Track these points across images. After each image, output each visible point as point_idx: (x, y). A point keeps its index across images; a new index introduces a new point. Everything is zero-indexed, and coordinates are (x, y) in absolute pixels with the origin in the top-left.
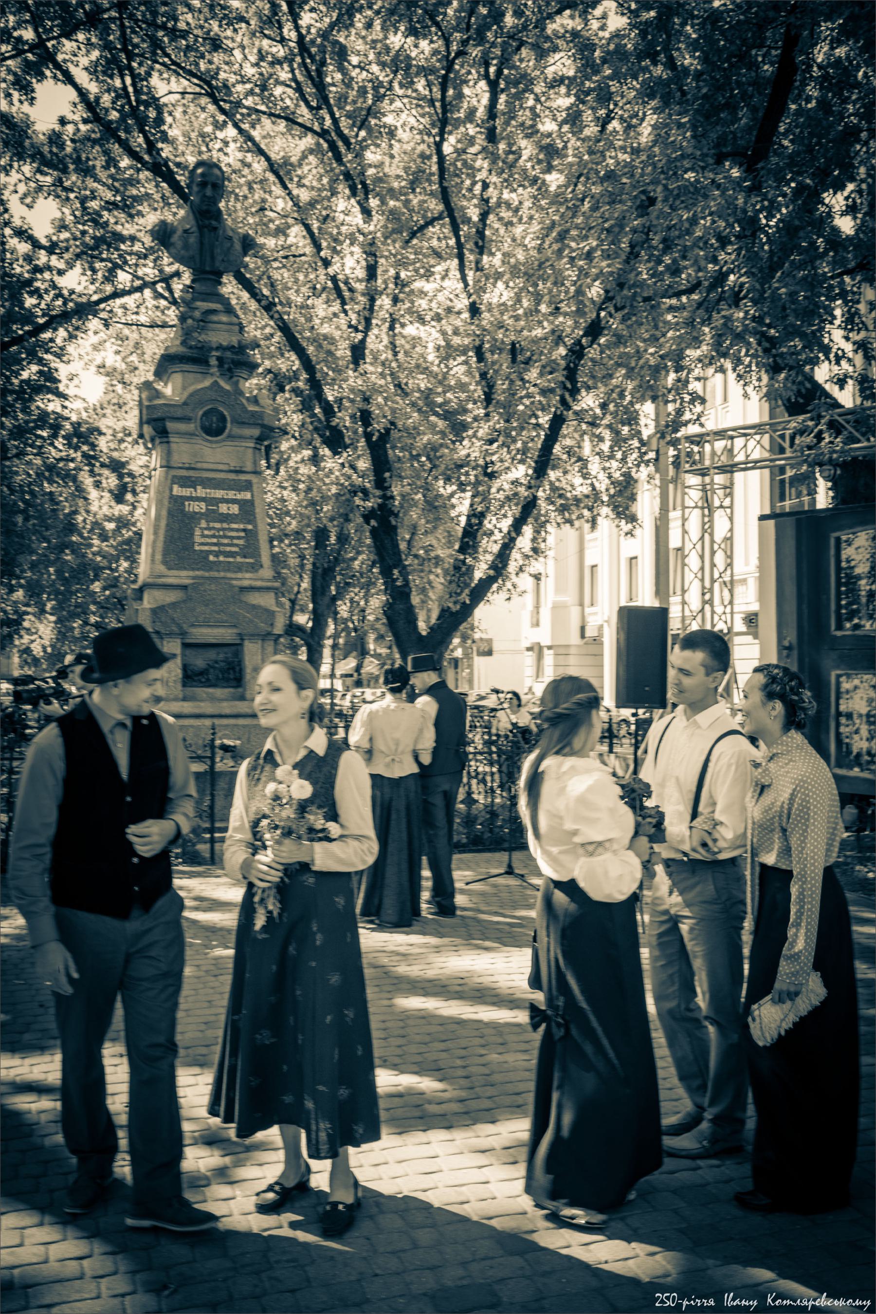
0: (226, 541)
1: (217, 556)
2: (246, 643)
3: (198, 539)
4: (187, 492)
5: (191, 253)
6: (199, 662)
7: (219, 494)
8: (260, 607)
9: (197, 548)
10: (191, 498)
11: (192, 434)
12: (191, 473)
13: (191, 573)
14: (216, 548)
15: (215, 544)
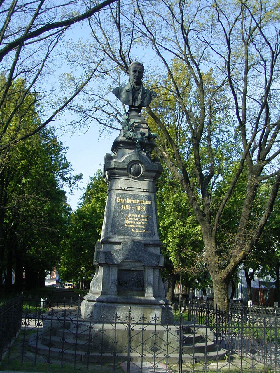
0: (139, 223)
1: (135, 230)
2: (146, 269)
3: (127, 222)
4: (123, 200)
7: (137, 202)
8: (153, 253)
12: (125, 192)
13: (123, 237)
15: (134, 224)
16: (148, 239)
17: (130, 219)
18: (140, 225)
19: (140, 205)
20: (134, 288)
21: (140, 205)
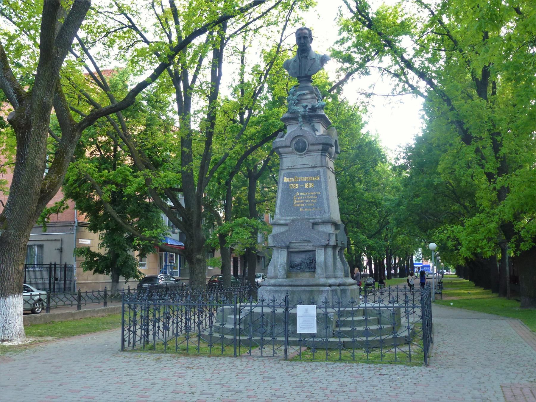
1: (304, 209)
3: (295, 201)
4: (290, 180)
5: (296, 70)
6: (297, 259)
7: (305, 179)
9: (294, 206)
10: (292, 183)
11: (292, 153)
12: (292, 171)
14: (303, 205)
15: (303, 203)
16: (318, 217)
17: (299, 198)
18: (309, 203)
19: (309, 182)
20: (306, 270)
21: (309, 182)
